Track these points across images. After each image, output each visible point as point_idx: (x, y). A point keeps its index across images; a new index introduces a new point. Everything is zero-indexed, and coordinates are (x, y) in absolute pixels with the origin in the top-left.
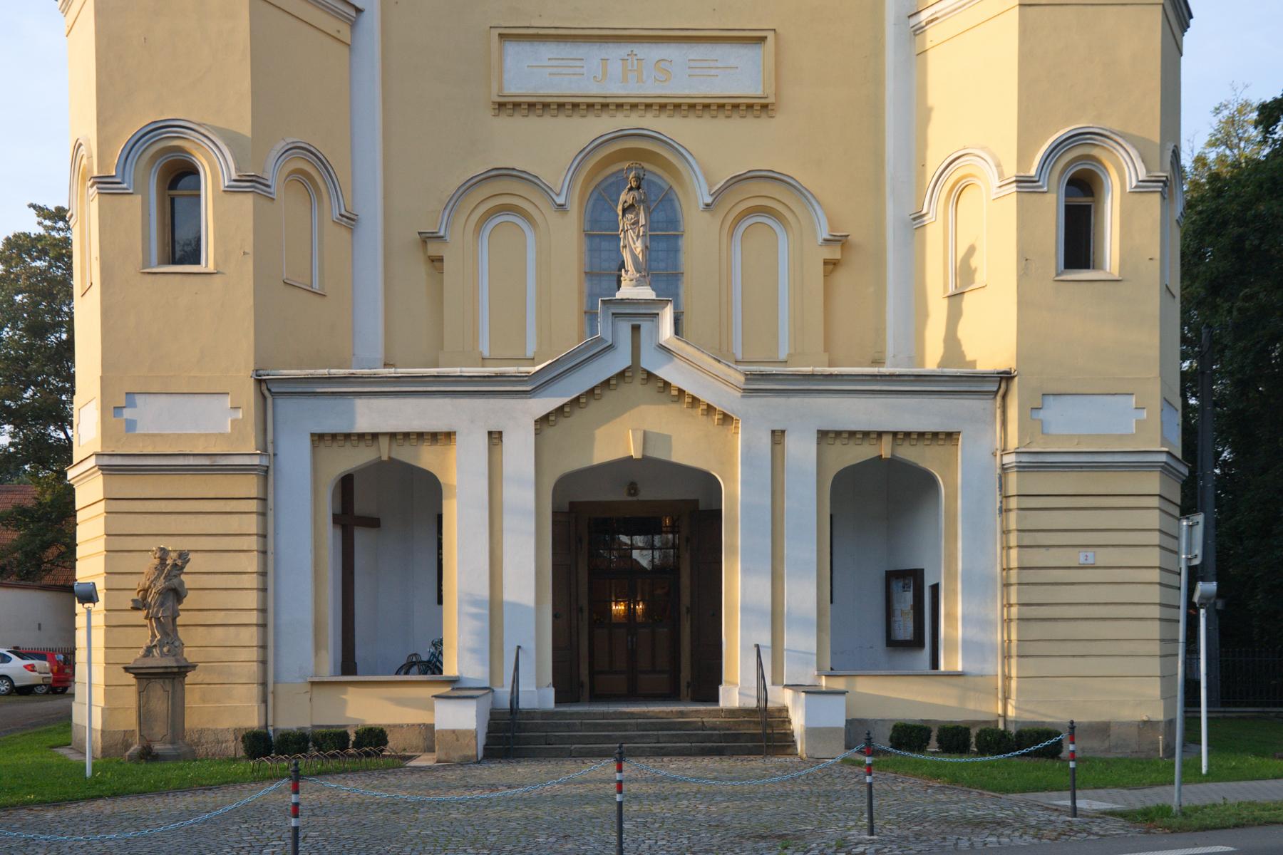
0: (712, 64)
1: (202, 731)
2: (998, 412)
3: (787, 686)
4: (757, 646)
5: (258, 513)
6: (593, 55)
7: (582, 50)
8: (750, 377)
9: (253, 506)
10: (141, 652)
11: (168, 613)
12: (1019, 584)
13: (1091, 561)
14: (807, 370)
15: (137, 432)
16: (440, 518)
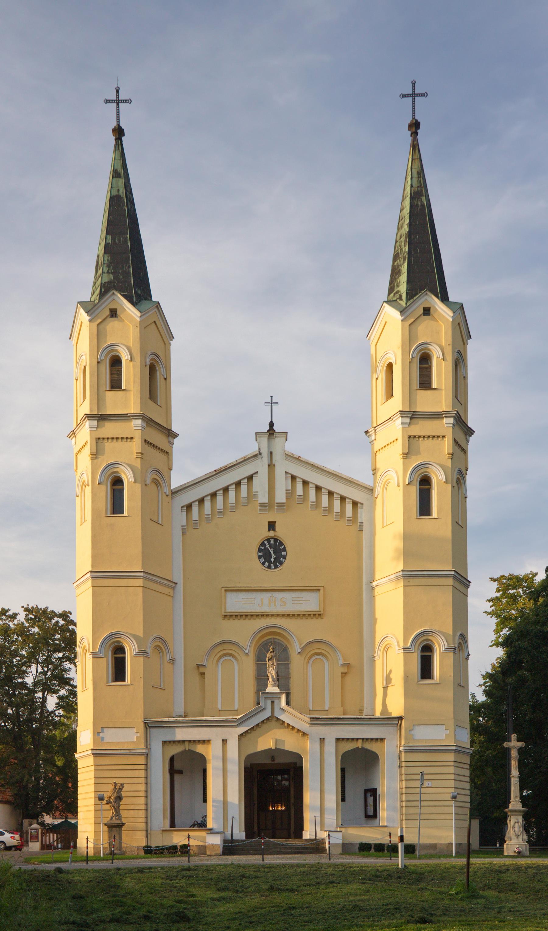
0: (300, 599)
1: (126, 847)
2: (398, 731)
3: (326, 831)
4: (315, 816)
5: (144, 770)
6: (258, 596)
7: (254, 595)
8: (312, 719)
9: (143, 767)
10: (109, 819)
11: (118, 805)
12: (406, 794)
13: (430, 785)
14: (332, 716)
15: (105, 741)
16: (205, 771)
